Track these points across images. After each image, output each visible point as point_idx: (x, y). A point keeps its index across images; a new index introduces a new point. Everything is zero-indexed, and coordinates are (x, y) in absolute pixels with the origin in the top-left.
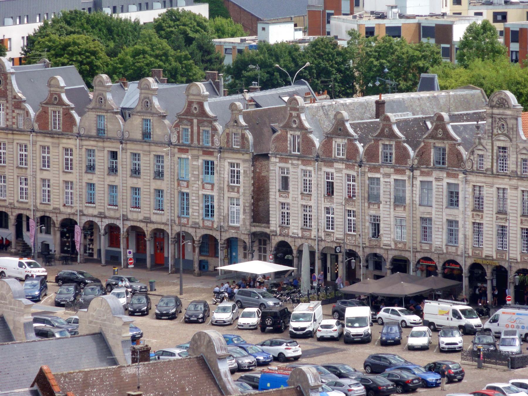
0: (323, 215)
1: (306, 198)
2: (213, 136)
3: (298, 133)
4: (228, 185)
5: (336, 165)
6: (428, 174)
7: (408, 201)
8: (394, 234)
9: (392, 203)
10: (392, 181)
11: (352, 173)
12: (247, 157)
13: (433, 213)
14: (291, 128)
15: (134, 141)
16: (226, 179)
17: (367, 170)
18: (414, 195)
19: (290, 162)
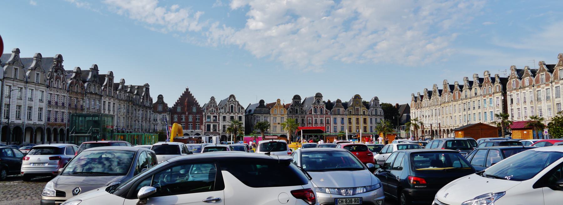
0: (524, 111)
1: (518, 105)
2: (491, 89)
3: (514, 80)
4: (496, 106)
5: (526, 89)
6: (558, 83)
7: (551, 98)
8: (548, 114)
9: (546, 100)
10: (545, 90)
11: (531, 90)
12: (501, 94)
13: (561, 100)
14: (512, 79)
15: (473, 97)
16: (496, 104)
17: (536, 88)
18: (553, 94)
19: (513, 92)
